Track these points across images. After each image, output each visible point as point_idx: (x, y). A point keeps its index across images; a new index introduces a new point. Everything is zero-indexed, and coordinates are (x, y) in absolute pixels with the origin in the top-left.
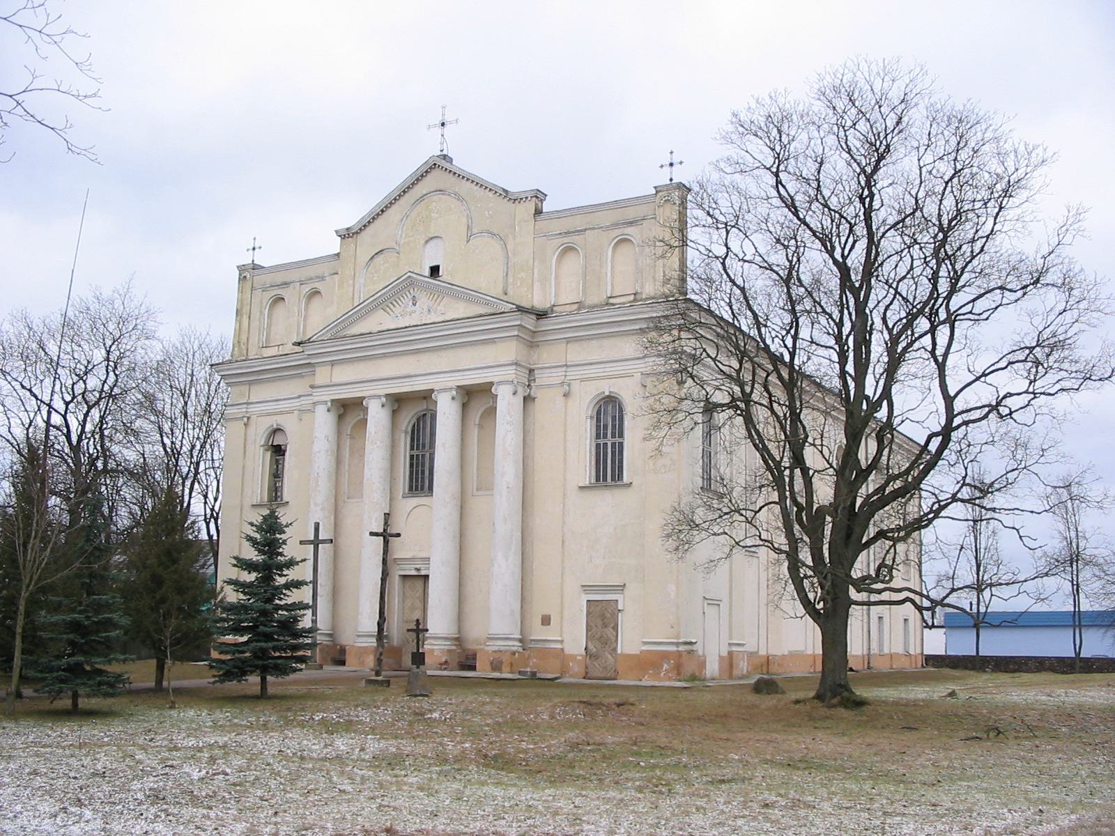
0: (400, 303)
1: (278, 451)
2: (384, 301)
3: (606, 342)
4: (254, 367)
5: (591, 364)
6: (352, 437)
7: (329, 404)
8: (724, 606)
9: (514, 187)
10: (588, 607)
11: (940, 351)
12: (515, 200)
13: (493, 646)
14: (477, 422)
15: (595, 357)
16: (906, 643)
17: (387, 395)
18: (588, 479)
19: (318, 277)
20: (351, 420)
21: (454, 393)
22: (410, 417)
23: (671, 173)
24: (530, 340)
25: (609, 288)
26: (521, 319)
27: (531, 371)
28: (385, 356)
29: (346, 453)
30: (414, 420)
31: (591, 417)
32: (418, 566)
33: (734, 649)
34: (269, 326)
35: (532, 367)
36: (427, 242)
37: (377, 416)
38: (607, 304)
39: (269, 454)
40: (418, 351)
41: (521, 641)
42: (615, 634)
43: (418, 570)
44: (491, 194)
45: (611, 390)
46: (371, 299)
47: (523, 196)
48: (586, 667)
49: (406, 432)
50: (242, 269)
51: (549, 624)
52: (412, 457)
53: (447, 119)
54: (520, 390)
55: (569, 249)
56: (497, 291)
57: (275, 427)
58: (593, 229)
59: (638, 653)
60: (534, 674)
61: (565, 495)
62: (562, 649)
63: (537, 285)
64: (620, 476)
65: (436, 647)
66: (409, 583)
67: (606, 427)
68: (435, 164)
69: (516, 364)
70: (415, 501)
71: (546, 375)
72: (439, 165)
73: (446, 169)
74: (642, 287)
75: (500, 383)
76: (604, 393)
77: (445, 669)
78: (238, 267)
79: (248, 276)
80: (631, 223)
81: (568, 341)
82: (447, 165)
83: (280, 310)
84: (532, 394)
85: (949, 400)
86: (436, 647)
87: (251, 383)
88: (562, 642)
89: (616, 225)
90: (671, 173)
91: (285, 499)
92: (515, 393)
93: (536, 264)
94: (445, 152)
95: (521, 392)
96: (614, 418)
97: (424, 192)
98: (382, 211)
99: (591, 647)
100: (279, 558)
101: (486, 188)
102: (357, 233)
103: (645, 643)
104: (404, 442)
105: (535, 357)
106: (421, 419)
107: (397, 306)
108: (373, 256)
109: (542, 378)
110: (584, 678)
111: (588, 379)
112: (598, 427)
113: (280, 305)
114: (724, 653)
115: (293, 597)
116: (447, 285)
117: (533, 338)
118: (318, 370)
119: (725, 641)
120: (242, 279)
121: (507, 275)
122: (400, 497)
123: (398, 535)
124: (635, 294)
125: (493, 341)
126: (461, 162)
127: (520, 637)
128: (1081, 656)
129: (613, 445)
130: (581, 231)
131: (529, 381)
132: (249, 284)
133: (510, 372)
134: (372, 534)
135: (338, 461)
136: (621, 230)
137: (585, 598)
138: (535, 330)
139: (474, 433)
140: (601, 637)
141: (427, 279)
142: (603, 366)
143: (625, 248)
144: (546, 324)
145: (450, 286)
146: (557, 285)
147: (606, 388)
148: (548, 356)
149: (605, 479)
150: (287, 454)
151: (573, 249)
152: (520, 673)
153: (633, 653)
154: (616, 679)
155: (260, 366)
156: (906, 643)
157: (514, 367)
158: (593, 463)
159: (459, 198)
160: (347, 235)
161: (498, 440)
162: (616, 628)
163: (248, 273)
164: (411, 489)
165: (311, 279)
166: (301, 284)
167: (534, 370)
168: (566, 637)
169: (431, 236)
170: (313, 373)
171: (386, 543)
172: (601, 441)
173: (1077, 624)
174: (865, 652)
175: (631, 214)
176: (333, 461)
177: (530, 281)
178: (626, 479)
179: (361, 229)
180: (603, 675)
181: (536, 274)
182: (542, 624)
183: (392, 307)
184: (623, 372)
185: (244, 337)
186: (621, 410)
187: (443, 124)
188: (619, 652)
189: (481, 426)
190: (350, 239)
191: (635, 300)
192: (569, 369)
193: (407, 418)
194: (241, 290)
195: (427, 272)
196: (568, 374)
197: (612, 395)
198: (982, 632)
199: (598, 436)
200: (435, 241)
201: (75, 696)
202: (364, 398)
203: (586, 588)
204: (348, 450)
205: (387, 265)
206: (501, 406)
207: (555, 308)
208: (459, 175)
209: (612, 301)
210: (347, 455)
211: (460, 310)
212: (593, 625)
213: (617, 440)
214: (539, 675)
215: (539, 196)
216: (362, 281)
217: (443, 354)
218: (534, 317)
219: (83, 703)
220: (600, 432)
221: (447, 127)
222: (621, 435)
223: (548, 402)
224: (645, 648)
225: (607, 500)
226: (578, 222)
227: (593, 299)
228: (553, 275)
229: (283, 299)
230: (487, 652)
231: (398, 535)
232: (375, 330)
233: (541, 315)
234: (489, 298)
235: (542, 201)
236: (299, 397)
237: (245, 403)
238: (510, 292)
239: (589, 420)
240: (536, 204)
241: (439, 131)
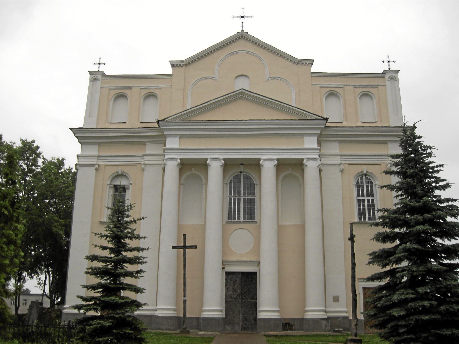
6: (184, 185)
7: (179, 161)
12: (298, 63)
17: (224, 160)
23: (389, 65)
30: (232, 177)
39: (112, 191)
45: (369, 171)
47: (304, 62)
52: (230, 199)
53: (245, 15)
57: (120, 173)
67: (363, 191)
68: (242, 36)
75: (308, 159)
76: (363, 172)
90: (389, 65)
96: (367, 187)
102: (186, 65)
118: (168, 140)
129: (368, 201)
147: (365, 169)
149: (365, 219)
164: (230, 218)
166: (141, 89)
172: (370, 198)
187: (243, 17)
193: (230, 175)
202: (207, 159)
221: (245, 20)
222: (372, 196)
241: (241, 20)
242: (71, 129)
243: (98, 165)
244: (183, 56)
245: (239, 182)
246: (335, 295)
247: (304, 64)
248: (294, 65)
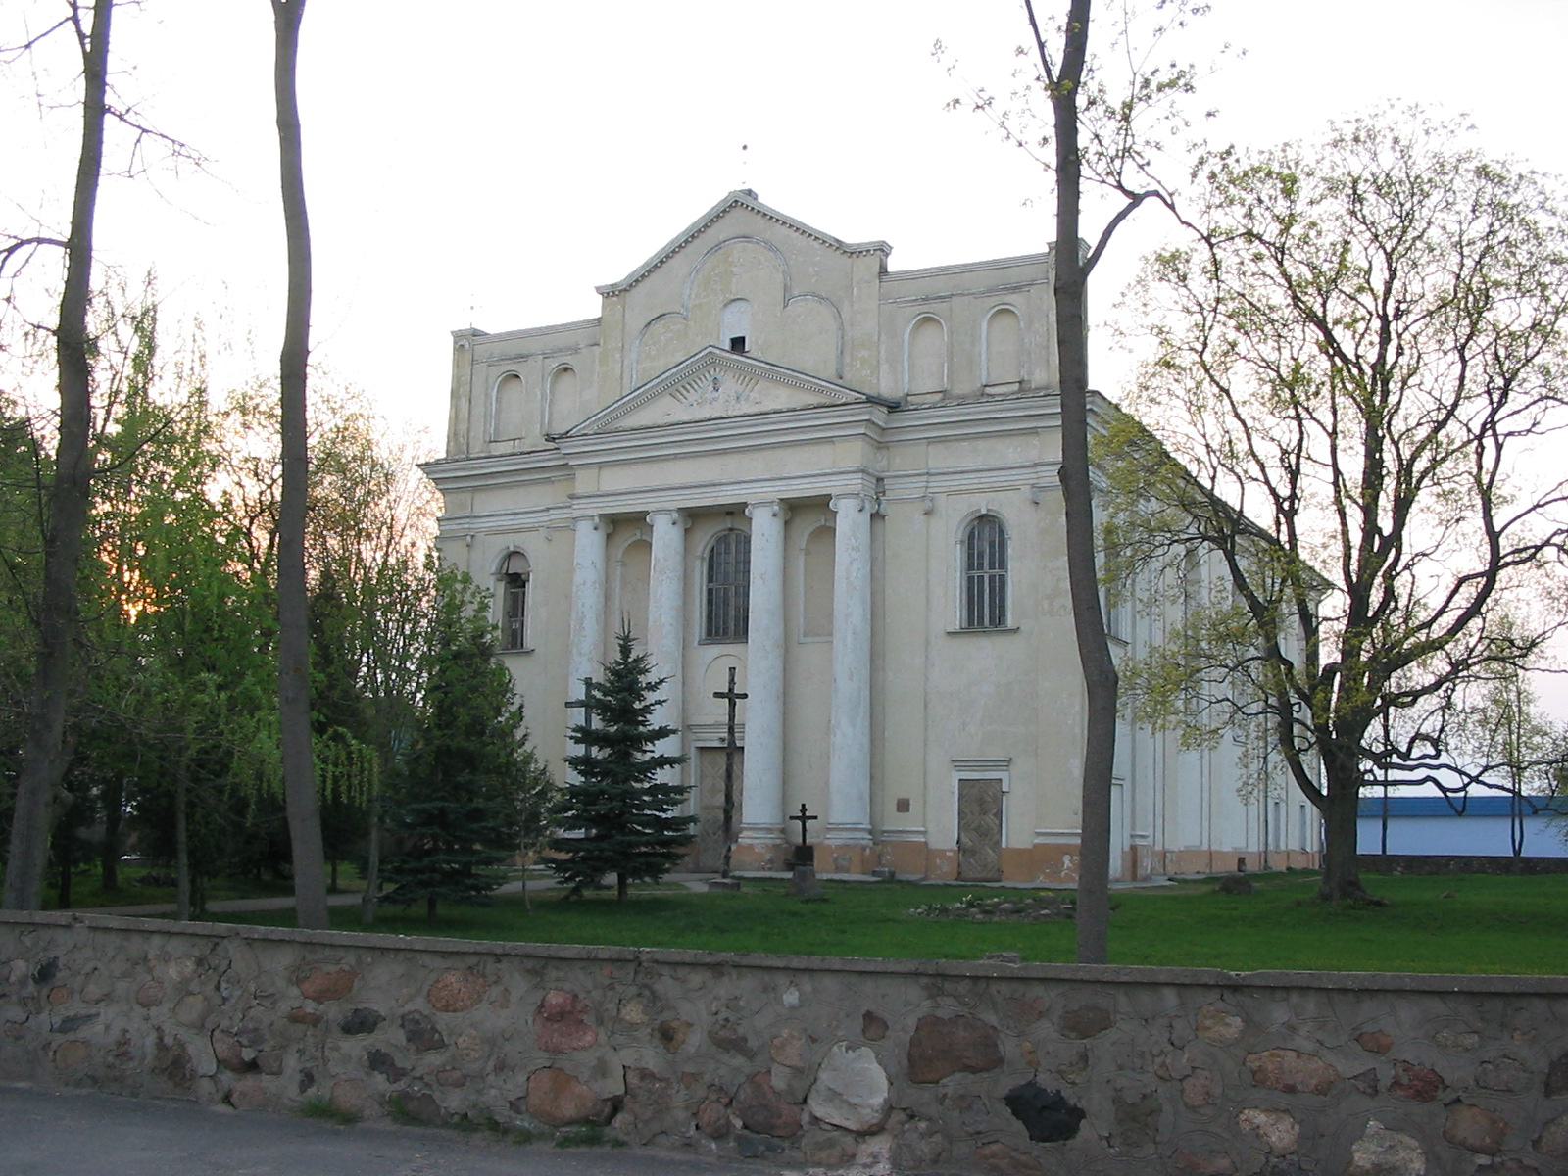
0: (696, 387)
1: (516, 582)
2: (676, 384)
3: (981, 444)
4: (482, 468)
5: (962, 473)
6: (624, 565)
7: (597, 520)
8: (1127, 785)
9: (851, 237)
11: (1485, 479)
13: (834, 840)
14: (803, 546)
15: (968, 463)
16: (1303, 838)
18: (958, 623)
19: (570, 349)
20: (626, 538)
21: (776, 508)
22: (710, 534)
24: (876, 437)
25: (984, 373)
26: (871, 413)
27: (880, 480)
28: (676, 456)
29: (617, 585)
31: (962, 542)
32: (722, 735)
33: (1139, 842)
34: (498, 411)
35: (883, 475)
36: (726, 305)
37: (665, 536)
38: (982, 395)
39: (502, 585)
40: (725, 451)
41: (870, 832)
42: (997, 822)
44: (816, 244)
46: (657, 381)
48: (959, 866)
49: (702, 558)
50: (458, 336)
51: (908, 811)
52: (710, 592)
54: (868, 505)
55: (928, 320)
56: (830, 373)
57: (512, 549)
58: (963, 295)
59: (1030, 846)
60: (892, 874)
61: (927, 643)
62: (926, 843)
63: (884, 367)
64: (998, 618)
66: (708, 756)
67: (981, 555)
68: (736, 201)
69: (863, 471)
70: (715, 650)
71: (897, 486)
72: (741, 204)
73: (753, 208)
74: (1030, 374)
76: (979, 510)
77: (770, 869)
78: (452, 333)
79: (467, 346)
80: (1016, 289)
81: (930, 441)
82: (749, 201)
83: (514, 390)
84: (882, 511)
85: (1493, 536)
86: (757, 841)
87: (476, 489)
88: (924, 833)
89: (991, 291)
91: (529, 643)
92: (861, 510)
93: (883, 338)
94: (745, 187)
95: (869, 508)
96: (992, 545)
97: (722, 238)
98: (662, 262)
99: (964, 839)
100: (641, 728)
101: (810, 235)
103: (1039, 834)
104: (700, 572)
105: (885, 462)
106: (723, 540)
107: (692, 391)
108: (649, 324)
109: (895, 489)
110: (957, 879)
111: (960, 492)
112: (970, 556)
113: (513, 385)
114: (1127, 848)
115: (664, 776)
116: (763, 365)
117: (881, 436)
118: (580, 475)
119: (1127, 835)
120: (459, 349)
121: (842, 352)
122: (696, 643)
123: (745, 696)
124: (1020, 382)
125: (829, 440)
126: (768, 199)
127: (869, 827)
128: (1522, 855)
129: (992, 579)
130: (944, 297)
131: (876, 493)
132: (468, 357)
133: (853, 482)
134: (717, 695)
135: (607, 597)
136: (997, 298)
137: (956, 777)
138: (884, 426)
139: (800, 562)
140: (980, 826)
141: (728, 355)
142: (979, 475)
143: (1006, 322)
144: (900, 420)
145: (768, 366)
146: (912, 366)
148: (902, 460)
150: (530, 587)
151: (934, 320)
152: (874, 873)
153: (1022, 847)
154: (999, 881)
155: (492, 467)
156: (1303, 838)
157: (860, 475)
158: (965, 601)
159: (771, 247)
160: (609, 293)
161: (840, 570)
162: (999, 815)
163: (468, 343)
164: (709, 633)
165: (560, 350)
167: (882, 479)
168: (932, 828)
169: (732, 297)
170: (572, 478)
171: (732, 705)
172: (976, 574)
173: (1517, 812)
174: (1262, 848)
175: (1014, 276)
176: (602, 599)
177: (875, 362)
178: (1010, 622)
179: (631, 285)
180: (983, 875)
181: (883, 352)
182: (898, 810)
183: (685, 392)
184: (1005, 484)
185: (463, 428)
186: (1002, 533)
188: (1004, 846)
189: (807, 552)
190: (615, 299)
191: (1021, 390)
192: (933, 479)
193: (704, 538)
194: (457, 364)
195: (727, 346)
196: (931, 485)
197: (991, 513)
198: (1390, 824)
199: (970, 567)
200: (738, 302)
201: (432, 904)
202: (647, 513)
203: (958, 764)
204: (618, 583)
205: (670, 335)
206: (842, 526)
207: (909, 398)
208: (772, 217)
209: (988, 390)
210: (618, 590)
211: (780, 398)
212: (967, 811)
213: (997, 572)
214: (900, 876)
215: (882, 249)
216: (634, 356)
217: (757, 455)
218: (885, 409)
219: (442, 910)
220: (972, 561)
222: (1003, 565)
223: (904, 521)
224: (1038, 840)
225: (985, 651)
226: (941, 287)
227: (963, 388)
228: (906, 356)
229: (518, 377)
230: (829, 846)
231: (745, 696)
232: (660, 423)
233: (893, 407)
234: (824, 384)
235: (887, 255)
236: (548, 509)
237: (468, 517)
238: (847, 376)
239: (959, 546)
240: (881, 260)
242: (419, 466)
243: (473, 536)
244: (618, 274)
245: (727, 552)
246: (903, 795)
248: (845, 256)
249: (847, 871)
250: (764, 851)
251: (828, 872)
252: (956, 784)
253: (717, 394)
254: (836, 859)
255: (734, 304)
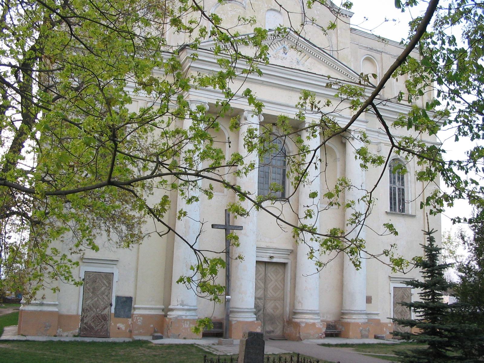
0: (275, 47)
10: (394, 292)
32: (272, 255)
36: (268, 10)
43: (271, 257)
65: (316, 321)
129: (399, 189)
140: (402, 311)
149: (395, 210)
169: (272, 7)
202: (243, 111)
230: (358, 323)
246: (369, 295)
247: (344, 15)
249: (367, 337)
250: (322, 327)
251: (357, 338)
252: (392, 289)
253: (286, 56)
254: (361, 330)
255: (271, 11)
